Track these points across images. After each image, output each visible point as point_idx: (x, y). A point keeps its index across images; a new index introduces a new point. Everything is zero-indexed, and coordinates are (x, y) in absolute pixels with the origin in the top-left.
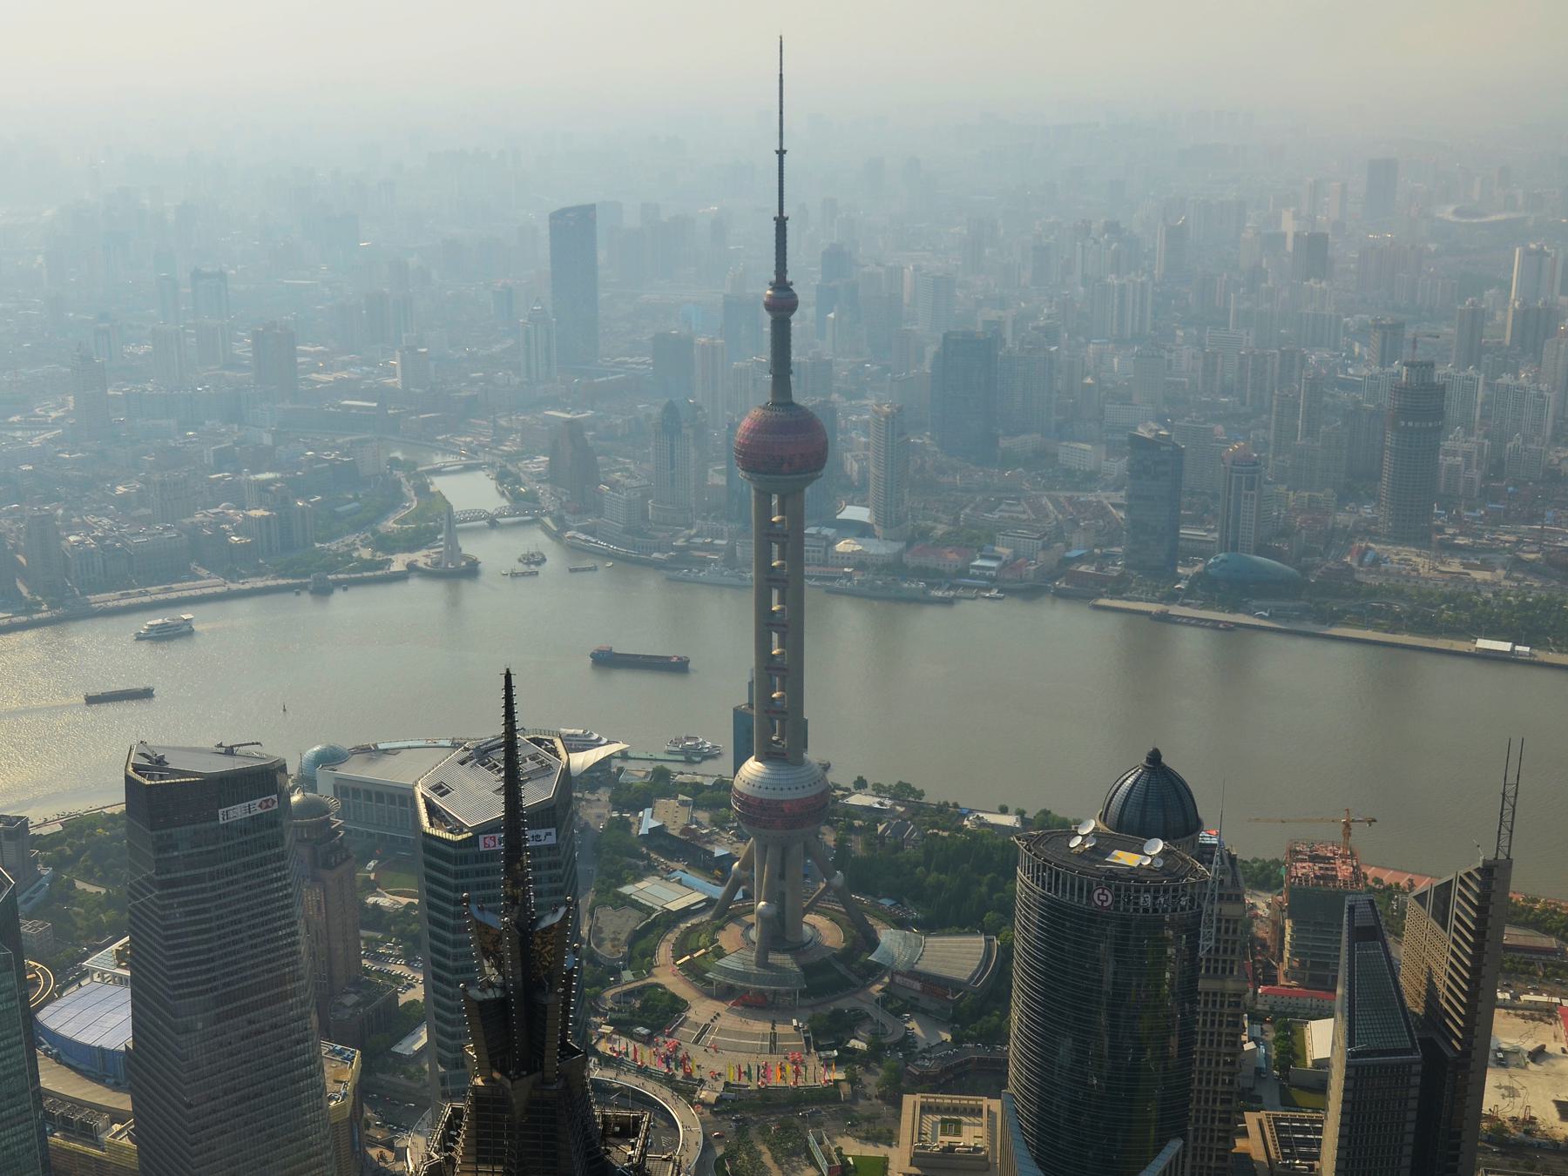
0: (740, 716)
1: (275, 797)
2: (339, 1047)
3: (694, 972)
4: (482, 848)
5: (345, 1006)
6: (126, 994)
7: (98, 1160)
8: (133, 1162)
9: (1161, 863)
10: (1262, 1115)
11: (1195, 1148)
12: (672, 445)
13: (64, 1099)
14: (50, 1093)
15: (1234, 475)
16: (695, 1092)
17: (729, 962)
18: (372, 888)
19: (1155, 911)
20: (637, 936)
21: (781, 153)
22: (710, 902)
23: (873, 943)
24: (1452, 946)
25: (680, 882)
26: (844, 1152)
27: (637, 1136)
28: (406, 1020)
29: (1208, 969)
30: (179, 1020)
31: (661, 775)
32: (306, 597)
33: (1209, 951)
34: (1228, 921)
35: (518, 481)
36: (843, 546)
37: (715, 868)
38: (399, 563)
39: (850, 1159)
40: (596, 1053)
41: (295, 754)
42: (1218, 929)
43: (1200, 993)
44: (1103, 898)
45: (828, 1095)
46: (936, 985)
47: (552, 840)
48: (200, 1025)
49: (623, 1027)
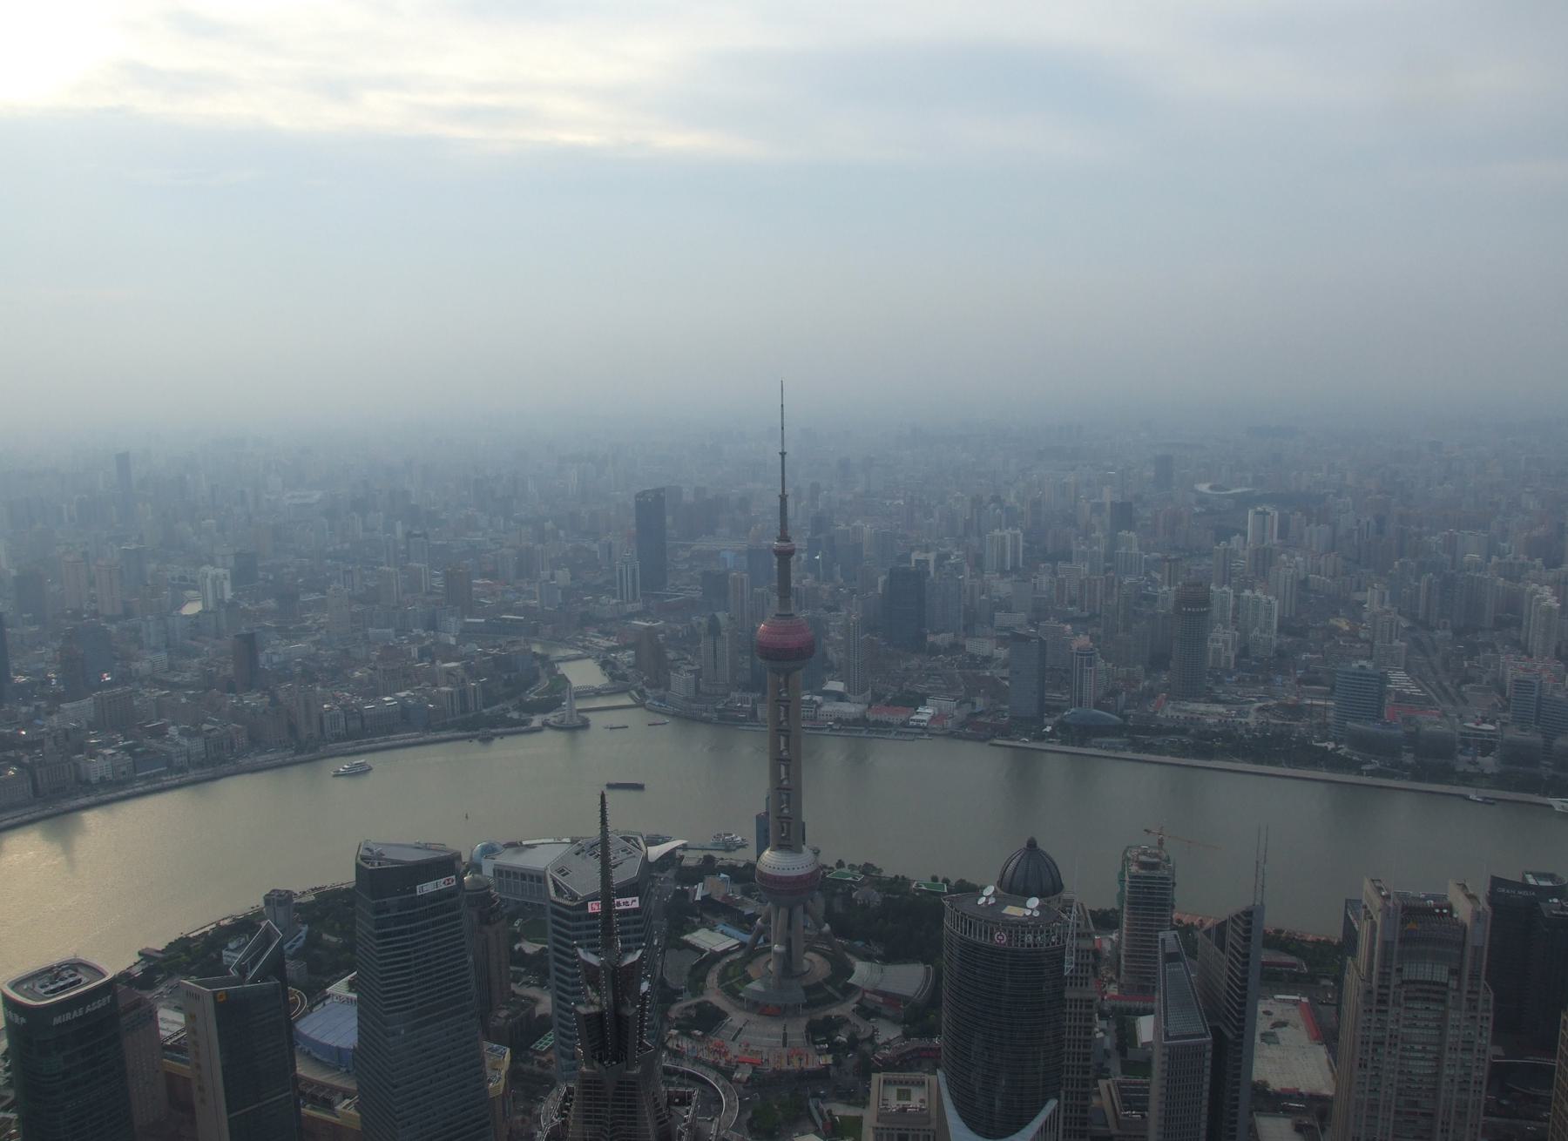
0: (761, 821)
1: (454, 877)
2: (495, 1046)
3: (732, 993)
4: (590, 911)
5: (499, 1018)
6: (354, 1010)
7: (335, 1125)
8: (357, 1126)
9: (1037, 914)
11: (1066, 1105)
12: (715, 643)
13: (310, 1083)
14: (302, 1078)
15: (1079, 657)
16: (733, 1073)
17: (756, 986)
18: (517, 937)
19: (1035, 945)
20: (695, 967)
21: (783, 454)
22: (742, 945)
23: (851, 972)
24: (1229, 964)
25: (722, 932)
26: (834, 1113)
27: (690, 1104)
28: (543, 1025)
29: (1071, 985)
30: (389, 1028)
31: (709, 860)
32: (476, 742)
33: (1072, 971)
34: (1083, 951)
35: (615, 667)
36: (826, 708)
37: (743, 922)
38: (537, 721)
39: (837, 1118)
40: (667, 1048)
41: (467, 846)
42: (1077, 958)
43: (1066, 1000)
44: (1001, 938)
45: (821, 1075)
46: (891, 999)
47: (636, 905)
48: (403, 1032)
49: (685, 1032)
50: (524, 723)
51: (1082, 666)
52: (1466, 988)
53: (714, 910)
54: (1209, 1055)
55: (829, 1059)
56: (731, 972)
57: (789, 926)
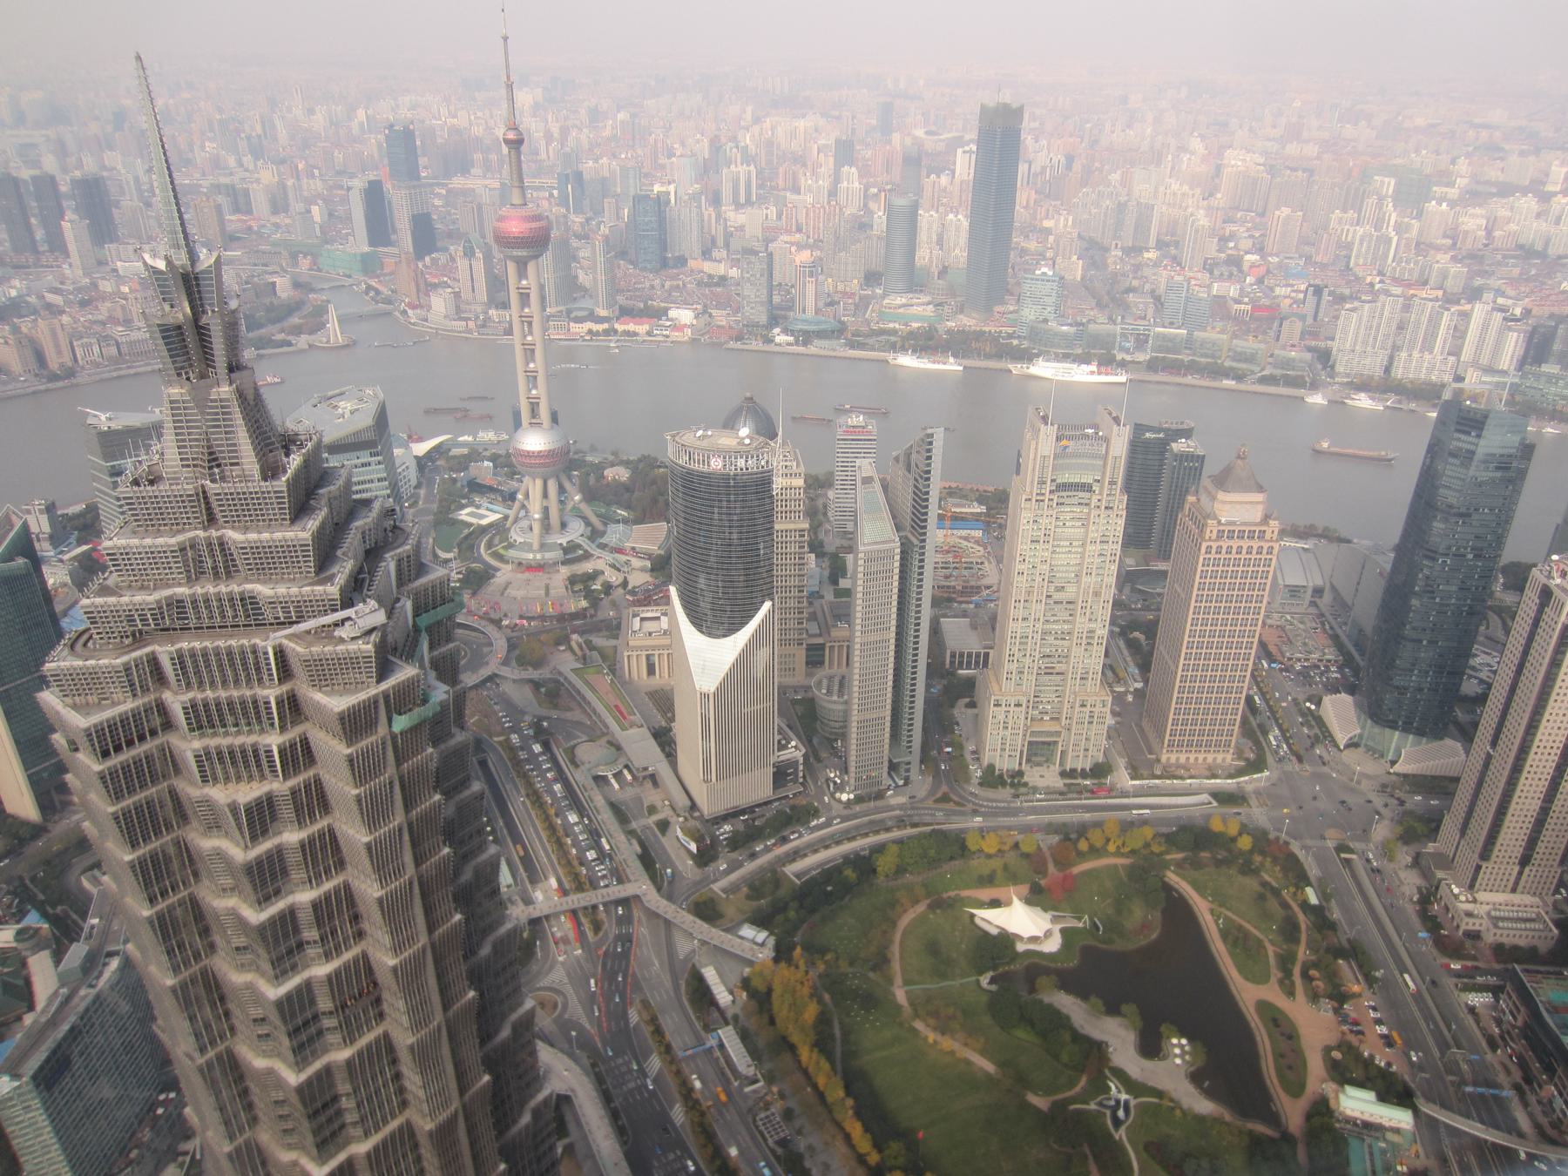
9: (747, 441)
10: (823, 601)
22: (506, 518)
23: (603, 534)
25: (488, 509)
38: (303, 341)
44: (716, 464)
45: (580, 615)
50: (290, 344)
51: (804, 277)
52: (1106, 492)
53: (476, 487)
54: (898, 557)
55: (584, 604)
56: (496, 541)
57: (545, 495)
